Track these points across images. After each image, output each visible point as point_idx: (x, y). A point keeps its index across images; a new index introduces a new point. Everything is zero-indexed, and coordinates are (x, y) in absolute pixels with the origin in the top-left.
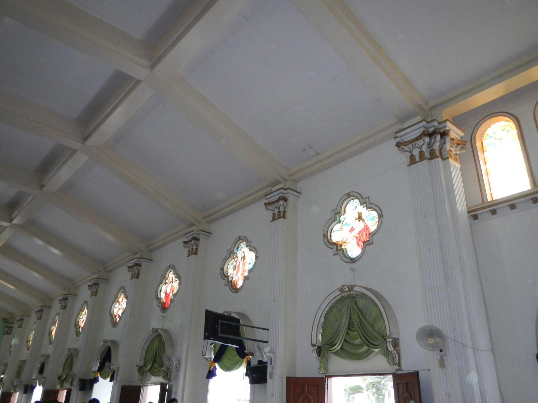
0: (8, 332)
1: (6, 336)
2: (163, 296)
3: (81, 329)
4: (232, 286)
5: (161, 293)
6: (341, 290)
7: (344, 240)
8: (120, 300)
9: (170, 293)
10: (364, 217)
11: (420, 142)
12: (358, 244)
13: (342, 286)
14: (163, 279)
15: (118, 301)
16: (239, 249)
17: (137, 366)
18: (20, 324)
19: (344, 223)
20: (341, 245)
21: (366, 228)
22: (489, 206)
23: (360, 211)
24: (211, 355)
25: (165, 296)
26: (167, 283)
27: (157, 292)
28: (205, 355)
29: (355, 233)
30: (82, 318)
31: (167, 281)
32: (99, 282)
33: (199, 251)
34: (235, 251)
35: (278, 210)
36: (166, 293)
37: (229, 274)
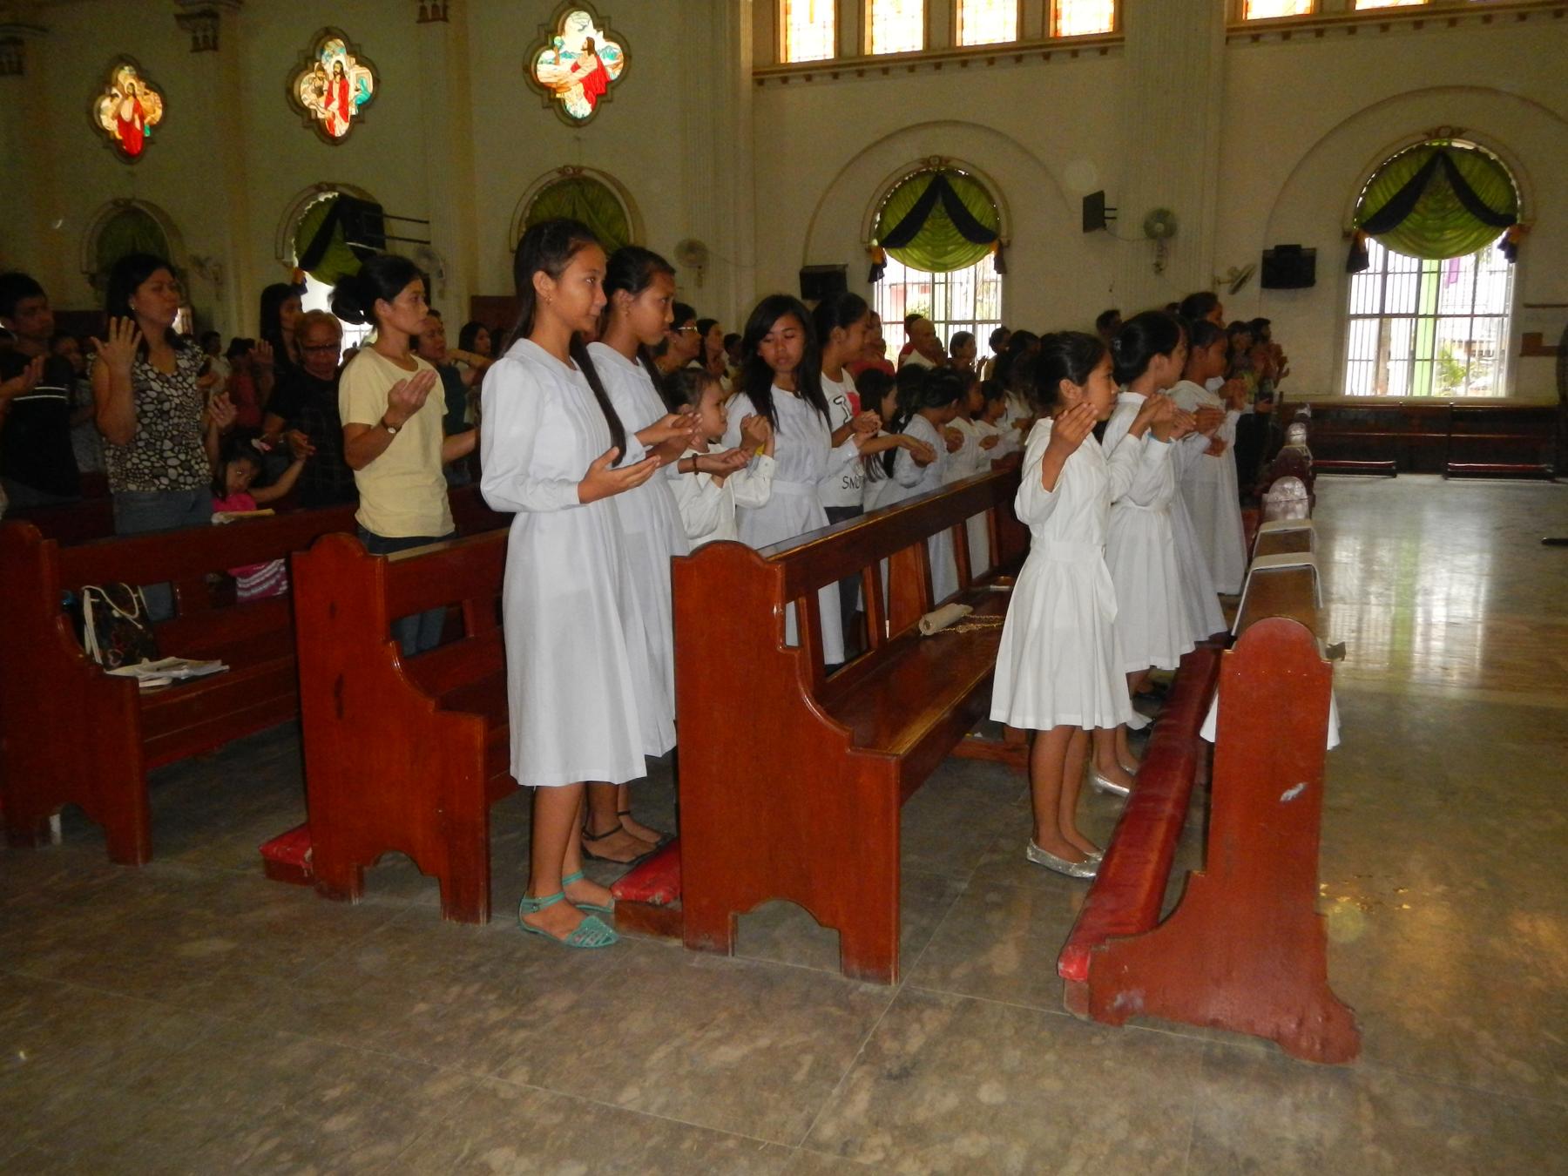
2: (109, 123)
4: (321, 130)
6: (562, 171)
7: (562, 82)
9: (133, 121)
10: (597, 47)
12: (586, 94)
13: (565, 167)
14: (104, 84)
16: (326, 53)
17: (83, 273)
19: (561, 52)
20: (555, 91)
21: (601, 69)
22: (781, 72)
24: (291, 257)
26: (116, 95)
27: (92, 114)
28: (283, 258)
29: (581, 74)
31: (115, 91)
34: (318, 58)
36: (118, 117)
37: (306, 103)
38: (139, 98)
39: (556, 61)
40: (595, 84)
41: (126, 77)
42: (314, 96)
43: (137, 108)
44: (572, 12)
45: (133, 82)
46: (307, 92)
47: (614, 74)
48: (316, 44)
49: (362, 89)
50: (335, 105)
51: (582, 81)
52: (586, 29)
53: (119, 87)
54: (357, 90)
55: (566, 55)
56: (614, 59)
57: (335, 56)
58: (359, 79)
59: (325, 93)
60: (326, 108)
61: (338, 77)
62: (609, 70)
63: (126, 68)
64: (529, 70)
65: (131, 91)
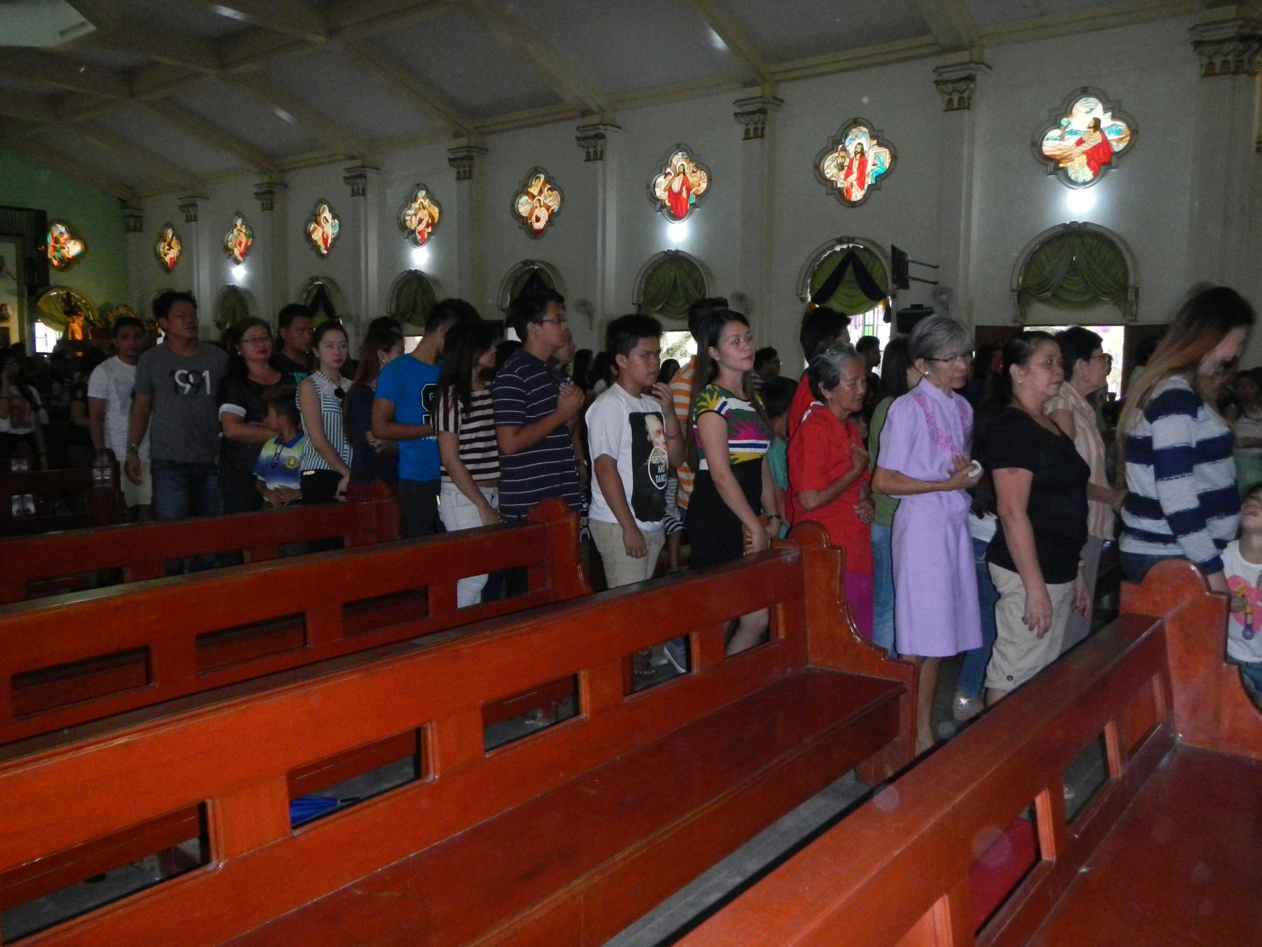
0: (135, 226)
1: (132, 237)
3: (417, 234)
4: (841, 195)
5: (656, 189)
7: (1065, 155)
8: (534, 190)
9: (681, 191)
11: (1228, 47)
12: (1089, 164)
14: (661, 165)
15: (528, 193)
16: (850, 137)
17: (634, 304)
18: (193, 213)
21: (1105, 143)
23: (1097, 116)
24: (806, 294)
25: (669, 196)
26: (669, 173)
30: (416, 215)
31: (668, 170)
32: (474, 154)
33: (766, 131)
34: (843, 142)
35: (960, 95)
37: (828, 176)
38: (688, 175)
39: (1062, 138)
40: (1098, 155)
41: (679, 160)
42: (835, 171)
43: (685, 182)
44: (1080, 99)
45: (685, 163)
46: (830, 168)
47: (1118, 147)
48: (843, 133)
49: (879, 163)
50: (854, 177)
51: (1085, 153)
52: (1093, 111)
53: (672, 166)
54: (874, 165)
55: (1072, 132)
56: (1119, 135)
57: (859, 139)
58: (876, 156)
59: (846, 168)
60: (845, 179)
61: (858, 156)
62: (1114, 144)
63: (680, 153)
64: (1037, 145)
65: (682, 170)
